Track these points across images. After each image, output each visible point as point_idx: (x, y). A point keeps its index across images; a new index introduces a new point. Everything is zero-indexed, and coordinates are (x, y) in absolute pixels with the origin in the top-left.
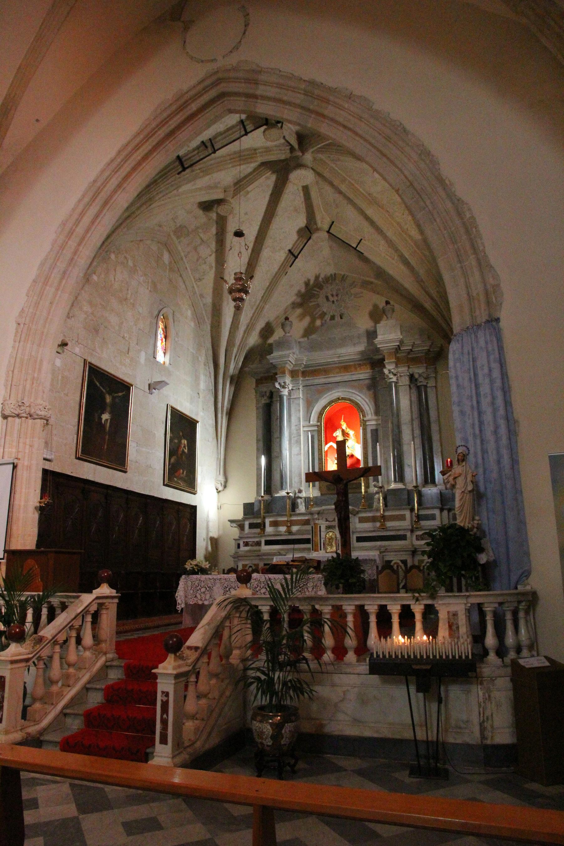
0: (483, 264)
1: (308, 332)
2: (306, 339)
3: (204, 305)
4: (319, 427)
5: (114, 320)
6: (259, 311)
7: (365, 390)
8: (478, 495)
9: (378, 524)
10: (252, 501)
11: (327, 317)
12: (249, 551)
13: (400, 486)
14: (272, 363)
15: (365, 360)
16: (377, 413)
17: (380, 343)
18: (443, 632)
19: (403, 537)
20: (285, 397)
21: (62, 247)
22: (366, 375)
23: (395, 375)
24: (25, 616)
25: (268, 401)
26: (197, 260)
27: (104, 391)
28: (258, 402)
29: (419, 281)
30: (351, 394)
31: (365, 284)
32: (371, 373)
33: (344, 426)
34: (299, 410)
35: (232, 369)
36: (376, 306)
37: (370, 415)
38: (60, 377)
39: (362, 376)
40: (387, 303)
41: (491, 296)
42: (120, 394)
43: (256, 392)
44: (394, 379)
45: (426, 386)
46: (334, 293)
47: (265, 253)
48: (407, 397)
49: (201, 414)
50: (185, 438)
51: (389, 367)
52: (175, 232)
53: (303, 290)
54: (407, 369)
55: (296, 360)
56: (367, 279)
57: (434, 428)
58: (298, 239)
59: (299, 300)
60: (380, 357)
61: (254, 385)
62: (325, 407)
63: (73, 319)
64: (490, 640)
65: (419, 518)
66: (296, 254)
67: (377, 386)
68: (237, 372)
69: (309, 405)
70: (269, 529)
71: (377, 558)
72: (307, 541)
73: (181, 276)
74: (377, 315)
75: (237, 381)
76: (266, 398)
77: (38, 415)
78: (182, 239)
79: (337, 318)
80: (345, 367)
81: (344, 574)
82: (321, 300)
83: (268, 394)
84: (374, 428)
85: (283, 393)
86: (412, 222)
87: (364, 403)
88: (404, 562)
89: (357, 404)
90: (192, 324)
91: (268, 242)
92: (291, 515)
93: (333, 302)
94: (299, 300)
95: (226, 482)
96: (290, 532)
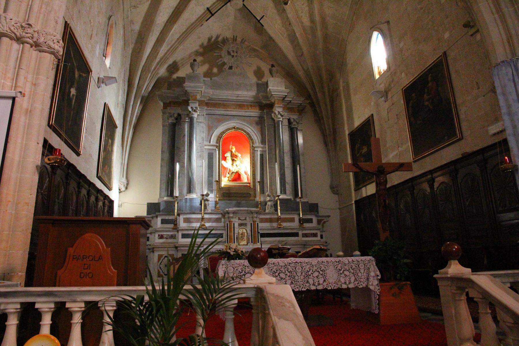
1: (208, 74)
3: (132, 30)
6: (173, 49)
7: (254, 125)
10: (155, 199)
12: (164, 243)
14: (186, 91)
15: (256, 102)
19: (296, 235)
22: (257, 114)
23: (282, 116)
24: (259, 323)
25: (175, 122)
29: (300, 56)
32: (259, 113)
36: (259, 68)
37: (257, 143)
39: (252, 114)
51: (278, 109)
53: (205, 44)
59: (201, 50)
66: (213, 13)
68: (147, 94)
69: (210, 129)
70: (182, 225)
75: (146, 102)
76: (173, 118)
77: (50, 47)
80: (241, 105)
82: (224, 53)
83: (176, 115)
85: (194, 116)
87: (253, 134)
89: (248, 134)
93: (233, 56)
94: (201, 50)
95: (128, 184)
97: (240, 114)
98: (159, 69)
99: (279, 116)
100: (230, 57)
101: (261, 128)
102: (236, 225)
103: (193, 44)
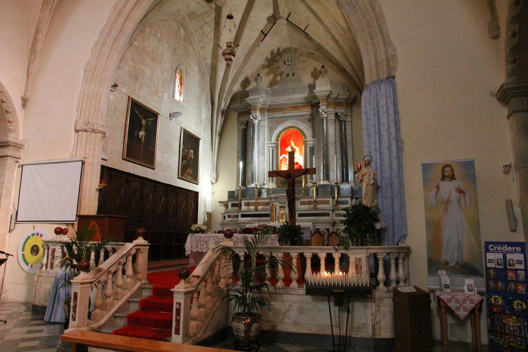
0: (387, 42)
1: (272, 84)
2: (270, 88)
4: (277, 144)
5: (148, 72)
6: (240, 70)
8: (376, 187)
9: (312, 206)
10: (233, 189)
11: (284, 75)
12: (231, 221)
13: (326, 183)
15: (307, 103)
16: (314, 136)
17: (318, 92)
18: (352, 270)
19: (327, 215)
20: (256, 125)
21: (115, 21)
23: (326, 113)
24: (90, 256)
25: (244, 127)
26: (202, 35)
27: (141, 117)
28: (238, 128)
29: (344, 54)
30: (298, 124)
31: (310, 55)
33: (293, 144)
34: (265, 134)
35: (223, 106)
36: (315, 69)
37: (309, 138)
38: (113, 107)
39: (305, 113)
40: (323, 67)
41: (390, 61)
42: (151, 119)
43: (238, 121)
44: (325, 115)
45: (345, 121)
46: (289, 60)
47: (246, 32)
48: (333, 127)
49: (203, 134)
50: (192, 149)
51: (322, 108)
52: (188, 16)
53: (269, 57)
54: (333, 109)
55: (264, 102)
56: (311, 51)
57: (349, 147)
58: (268, 23)
59: (267, 63)
60: (317, 101)
61: (237, 117)
62: (281, 132)
63: (121, 70)
64: (381, 276)
65: (338, 202)
67: (314, 120)
68: (226, 108)
69: (271, 130)
70: (244, 208)
71: (311, 227)
72: (267, 215)
73: (191, 45)
74: (316, 75)
75: (226, 114)
76: (244, 125)
77: (98, 130)
78: (193, 20)
79: (291, 76)
80: (295, 107)
81: (291, 234)
82: (281, 64)
83: (245, 123)
84: (312, 146)
86: (341, 15)
88: (328, 230)
89: (301, 131)
90: (198, 76)
91: (248, 25)
92: (258, 199)
93: (289, 65)
94: (267, 63)
95: (217, 177)
96: (257, 210)
97: (295, 114)
98: (232, 87)
99: (323, 113)
100: (286, 66)
101: (313, 124)
102: (278, 208)
103: (259, 59)
